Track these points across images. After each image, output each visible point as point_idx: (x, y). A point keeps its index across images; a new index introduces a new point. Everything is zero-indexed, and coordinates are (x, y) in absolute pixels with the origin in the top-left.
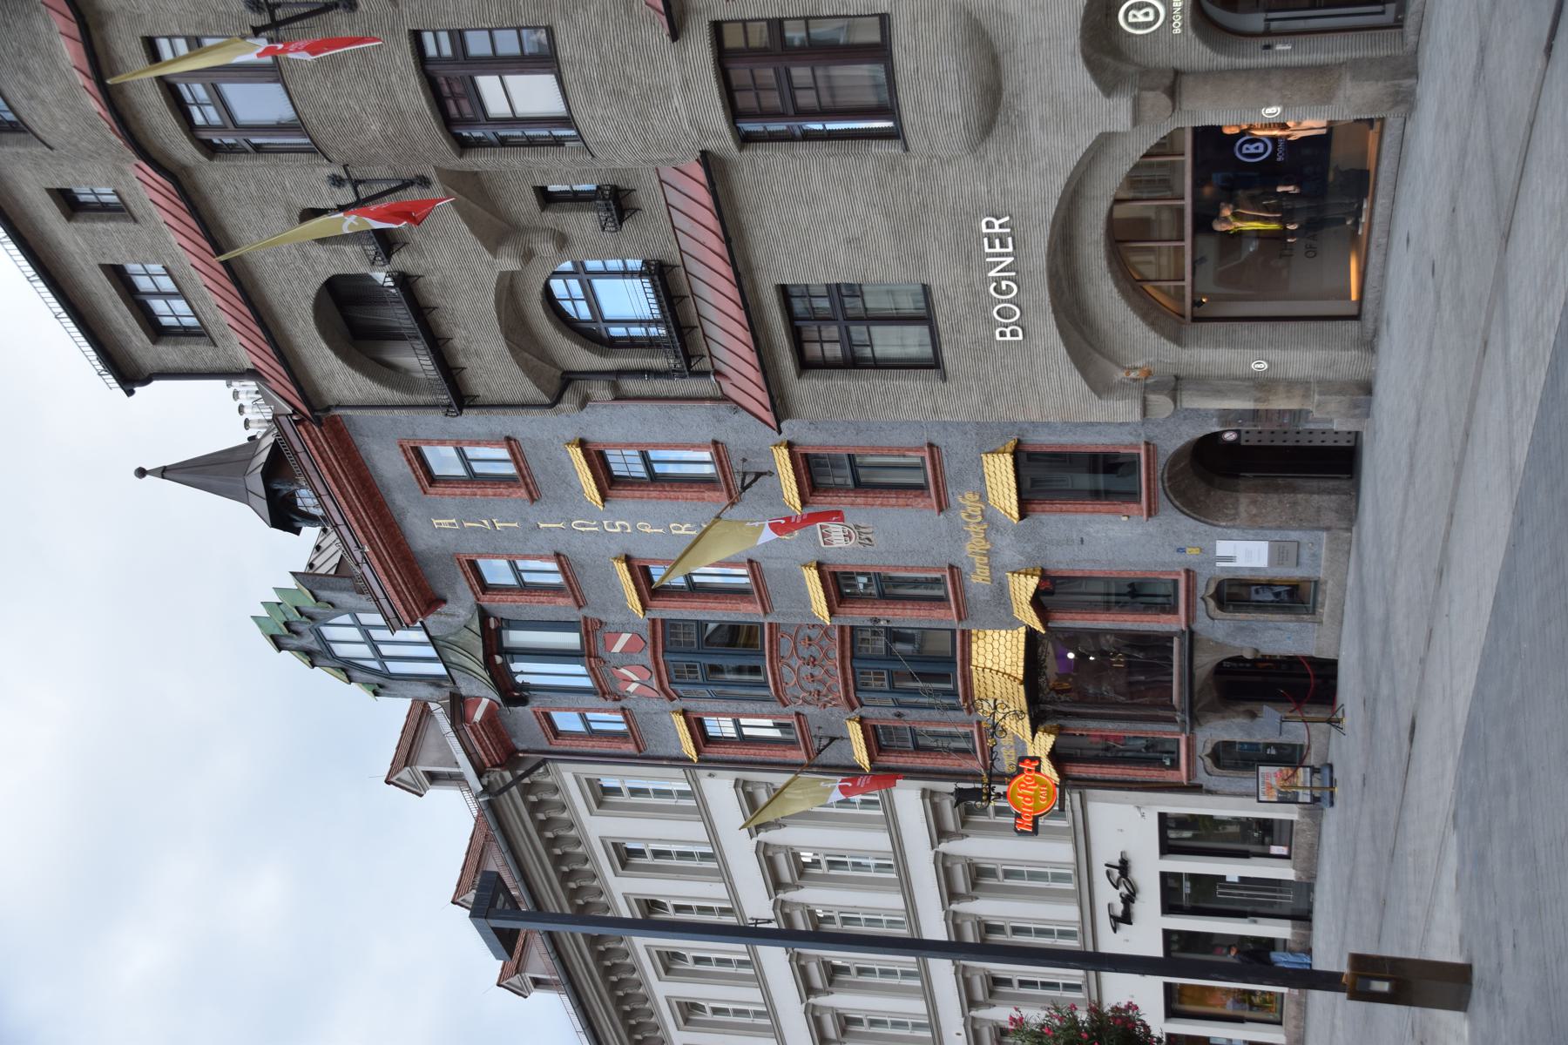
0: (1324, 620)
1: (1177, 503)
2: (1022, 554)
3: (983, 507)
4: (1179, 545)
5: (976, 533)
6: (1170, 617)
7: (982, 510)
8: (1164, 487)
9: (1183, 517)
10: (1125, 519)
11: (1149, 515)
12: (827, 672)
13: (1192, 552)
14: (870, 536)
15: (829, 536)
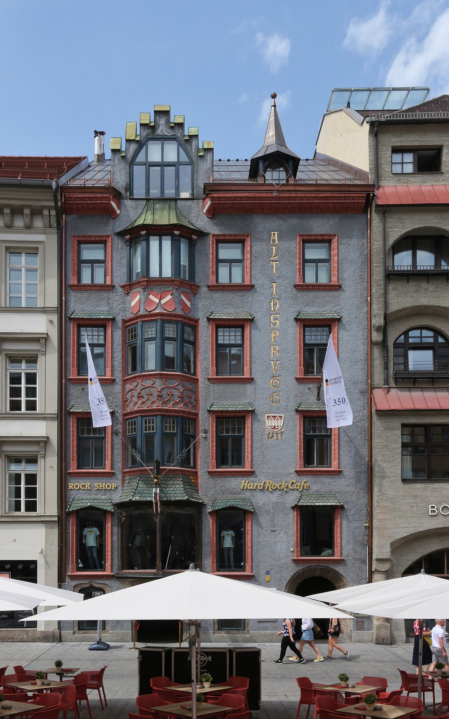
0: (216, 634)
1: (301, 572)
2: (264, 504)
3: (299, 490)
4: (272, 572)
5: (280, 486)
6: (215, 567)
7: (297, 489)
8: (312, 566)
9: (292, 574)
10: (292, 550)
11: (294, 560)
12: (176, 403)
13: (268, 578)
14: (275, 437)
15: (274, 419)
